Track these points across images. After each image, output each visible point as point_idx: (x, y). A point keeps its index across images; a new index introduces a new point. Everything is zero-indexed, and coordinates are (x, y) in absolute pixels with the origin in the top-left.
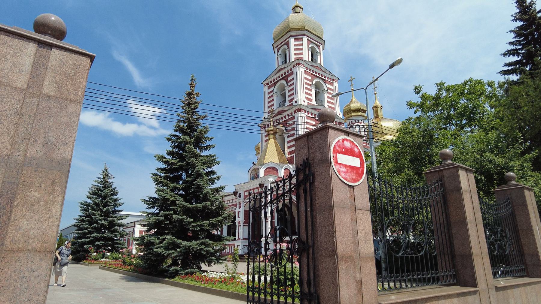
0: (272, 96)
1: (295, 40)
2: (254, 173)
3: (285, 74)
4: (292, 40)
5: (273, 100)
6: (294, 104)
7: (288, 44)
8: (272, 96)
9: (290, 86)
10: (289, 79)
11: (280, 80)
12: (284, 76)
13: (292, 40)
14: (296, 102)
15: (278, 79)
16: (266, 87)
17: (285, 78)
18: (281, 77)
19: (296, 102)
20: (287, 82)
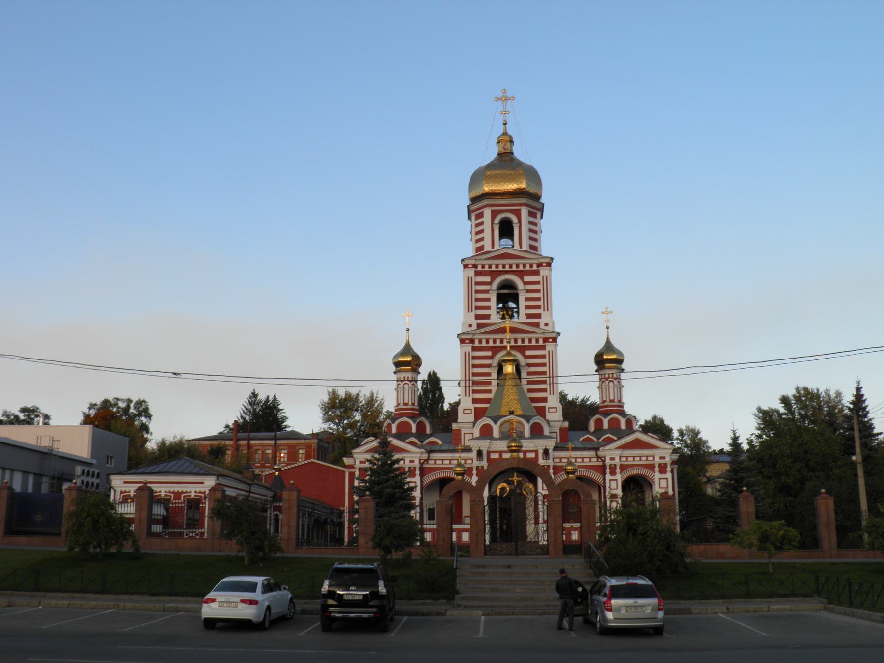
0: (487, 291)
1: (532, 214)
2: (507, 425)
3: (518, 266)
4: (524, 211)
5: (488, 300)
6: (542, 326)
7: (518, 213)
8: (487, 291)
9: (528, 291)
10: (527, 279)
11: (506, 272)
12: (514, 268)
13: (524, 211)
14: (546, 324)
15: (500, 268)
16: (471, 272)
17: (521, 274)
18: (507, 268)
19: (546, 324)
20: (526, 283)
